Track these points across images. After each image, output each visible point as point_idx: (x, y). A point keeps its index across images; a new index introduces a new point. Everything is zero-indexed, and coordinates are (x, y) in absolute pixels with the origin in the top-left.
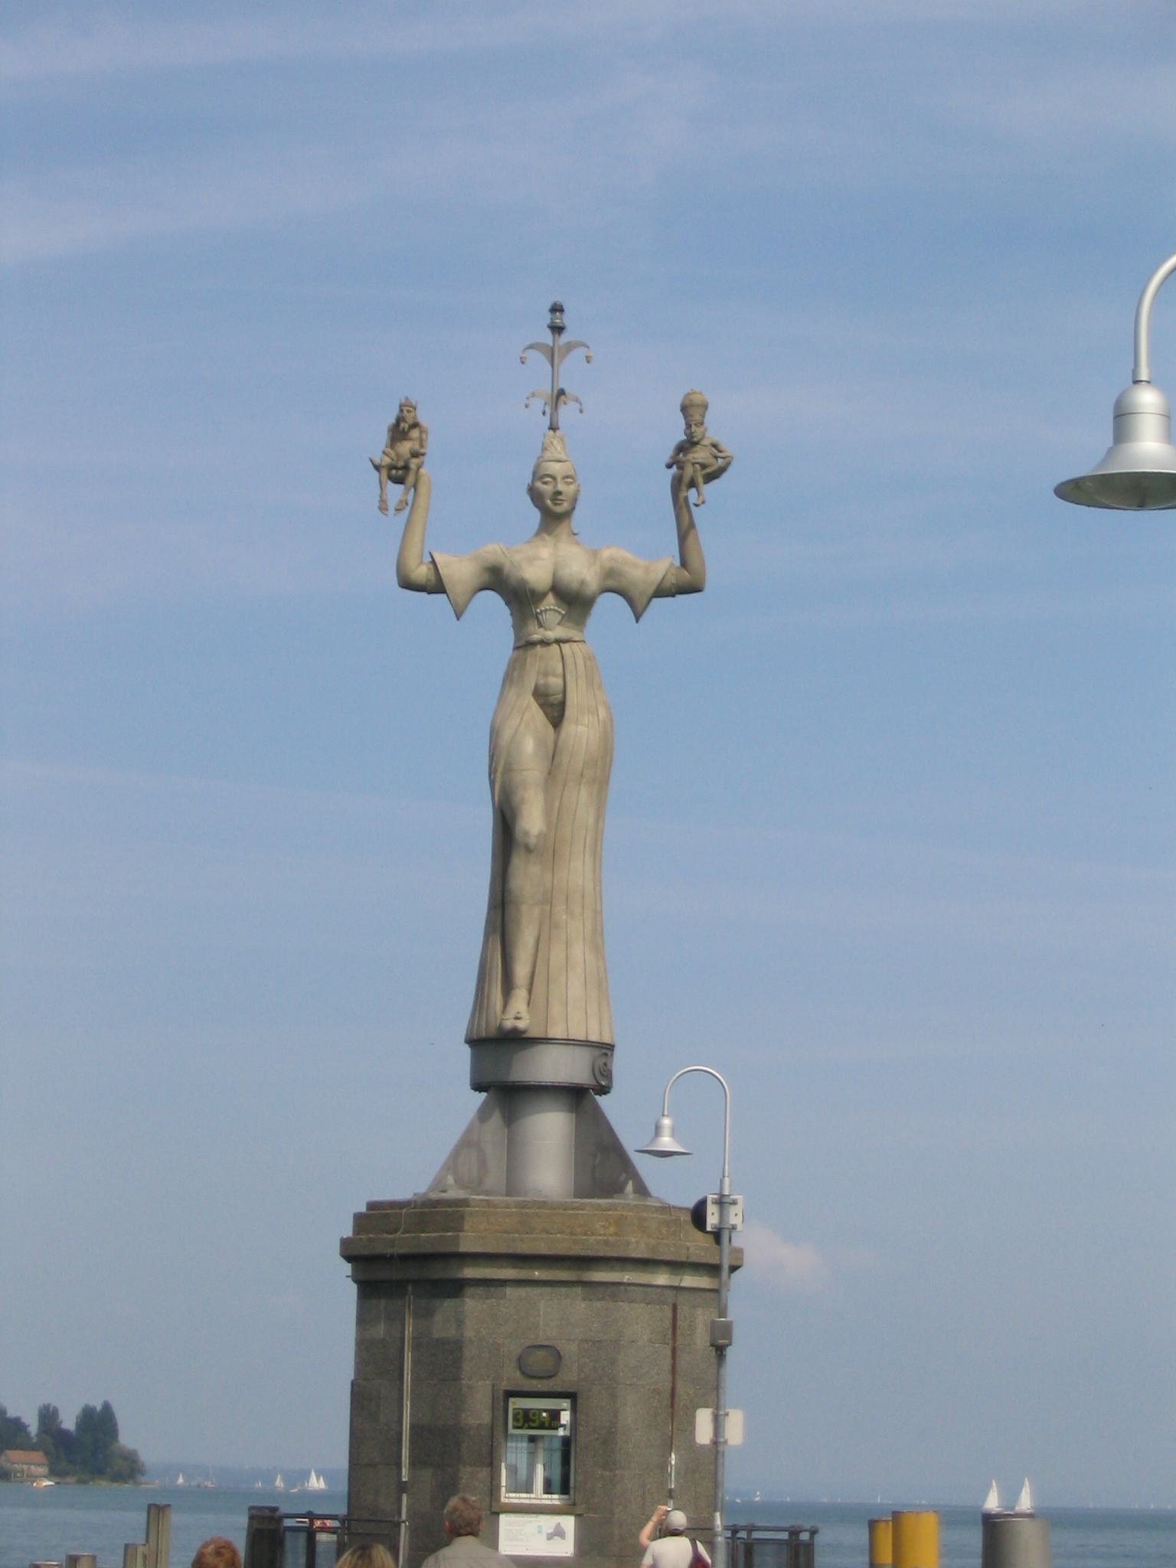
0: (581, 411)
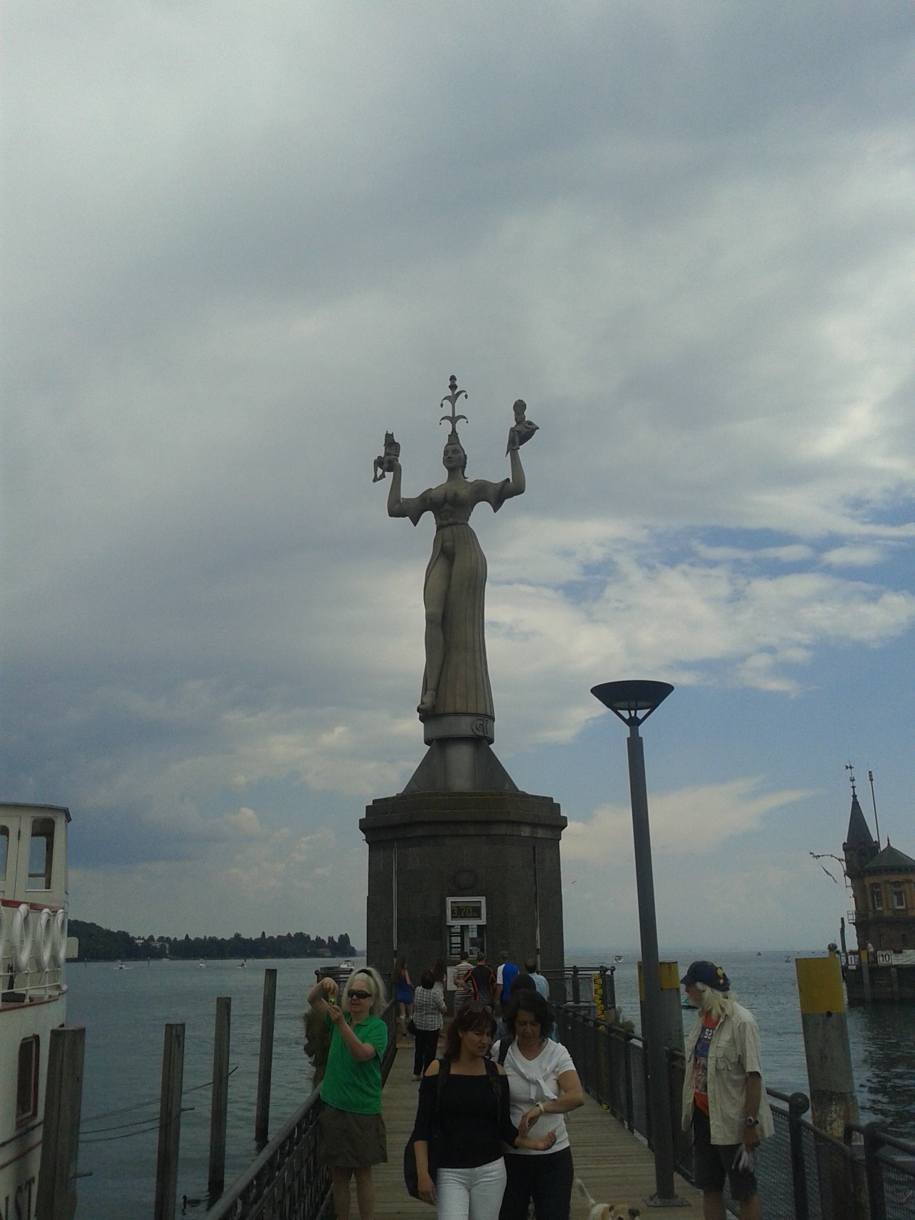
0: (467, 422)
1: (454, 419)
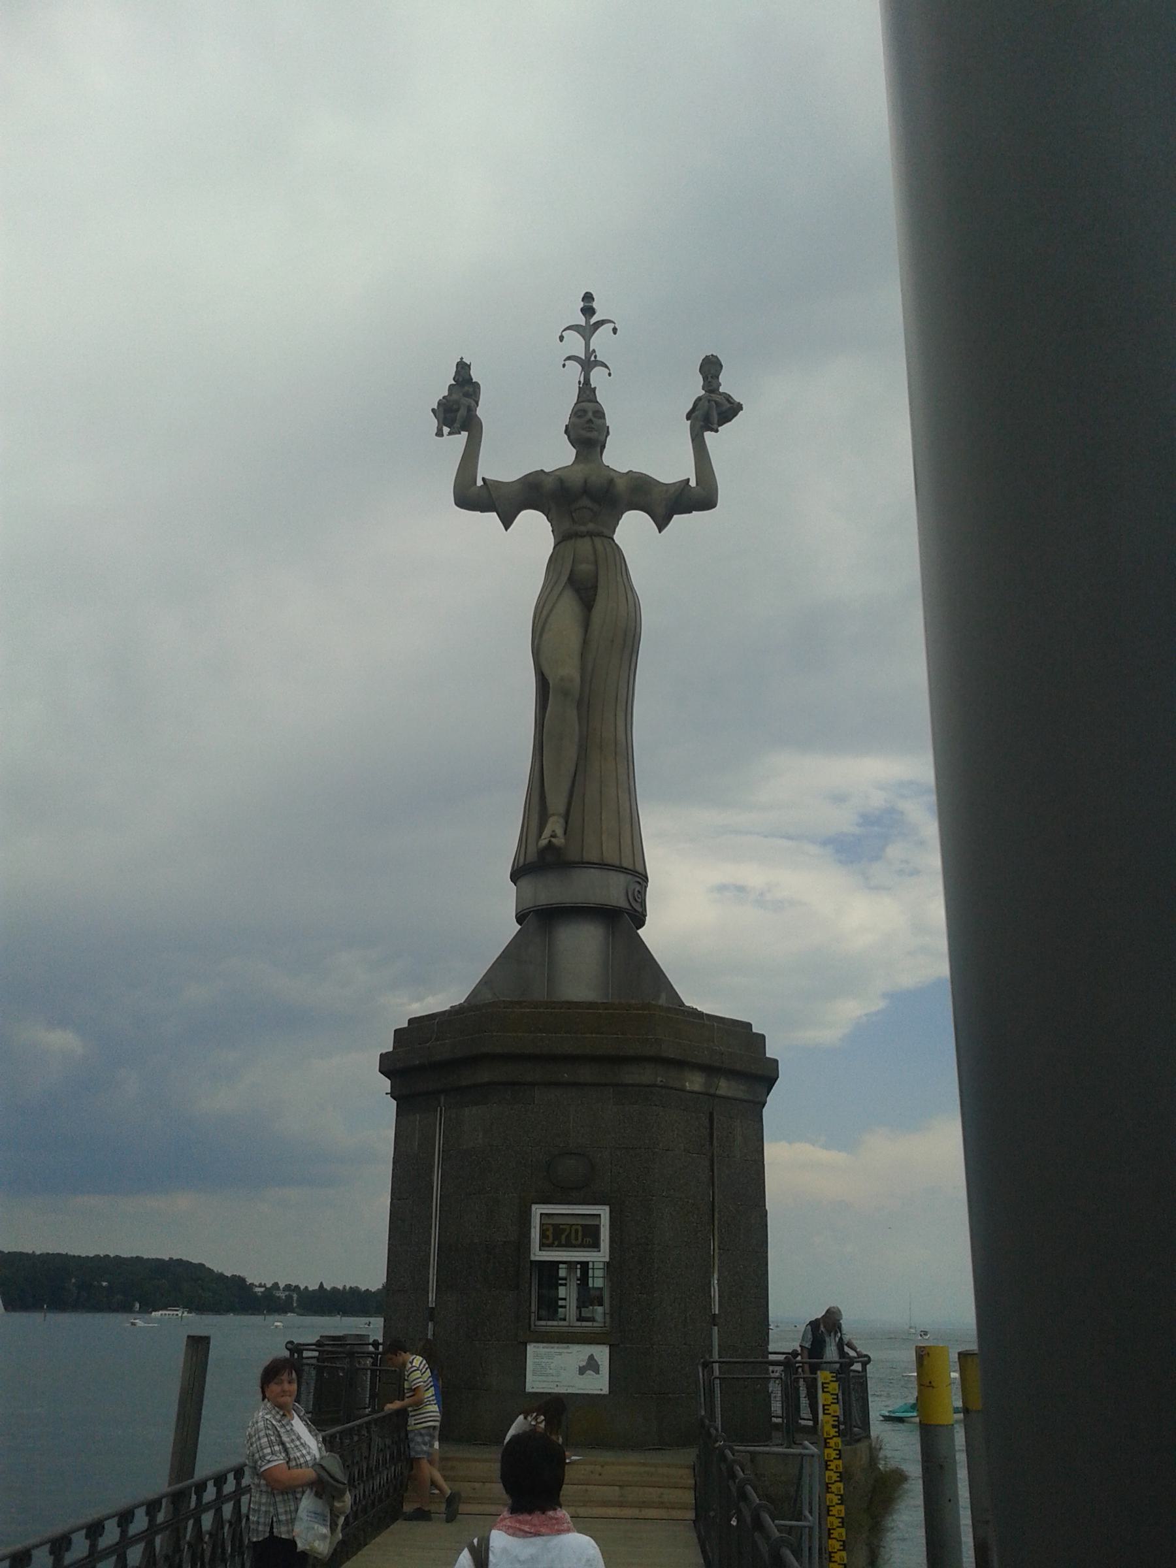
0: (610, 375)
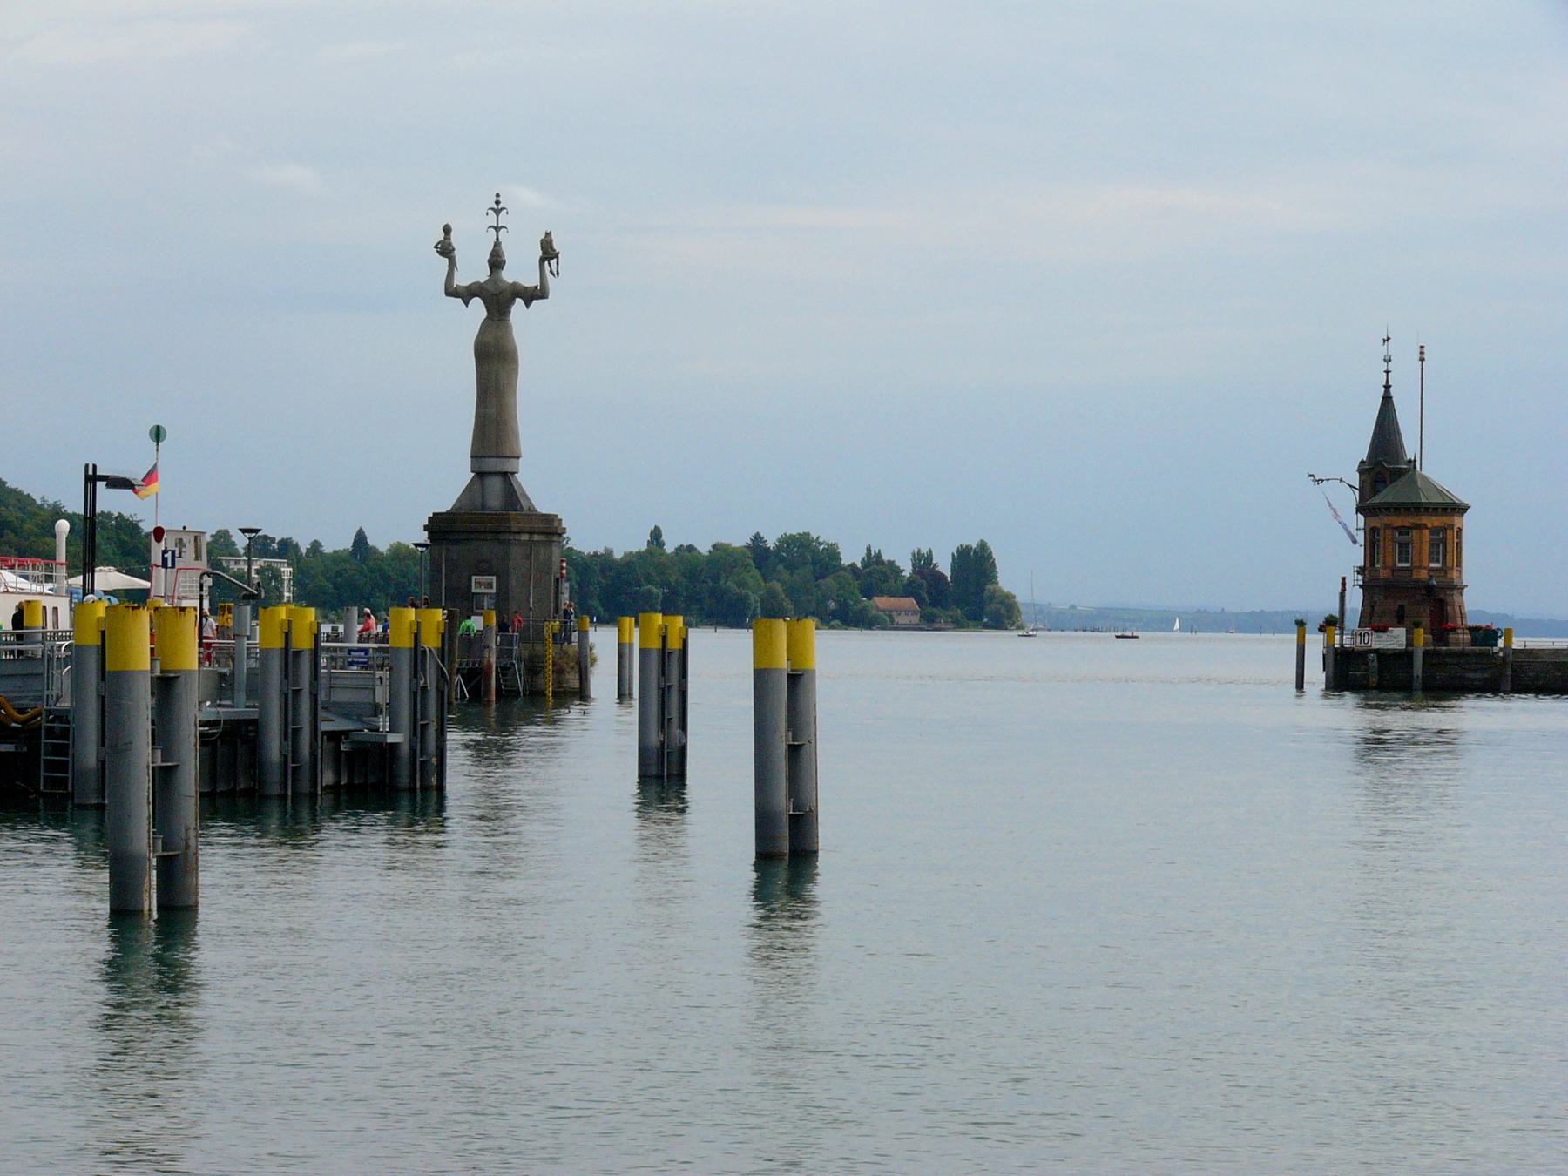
1: (497, 229)
